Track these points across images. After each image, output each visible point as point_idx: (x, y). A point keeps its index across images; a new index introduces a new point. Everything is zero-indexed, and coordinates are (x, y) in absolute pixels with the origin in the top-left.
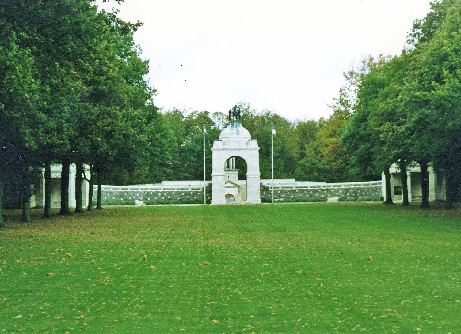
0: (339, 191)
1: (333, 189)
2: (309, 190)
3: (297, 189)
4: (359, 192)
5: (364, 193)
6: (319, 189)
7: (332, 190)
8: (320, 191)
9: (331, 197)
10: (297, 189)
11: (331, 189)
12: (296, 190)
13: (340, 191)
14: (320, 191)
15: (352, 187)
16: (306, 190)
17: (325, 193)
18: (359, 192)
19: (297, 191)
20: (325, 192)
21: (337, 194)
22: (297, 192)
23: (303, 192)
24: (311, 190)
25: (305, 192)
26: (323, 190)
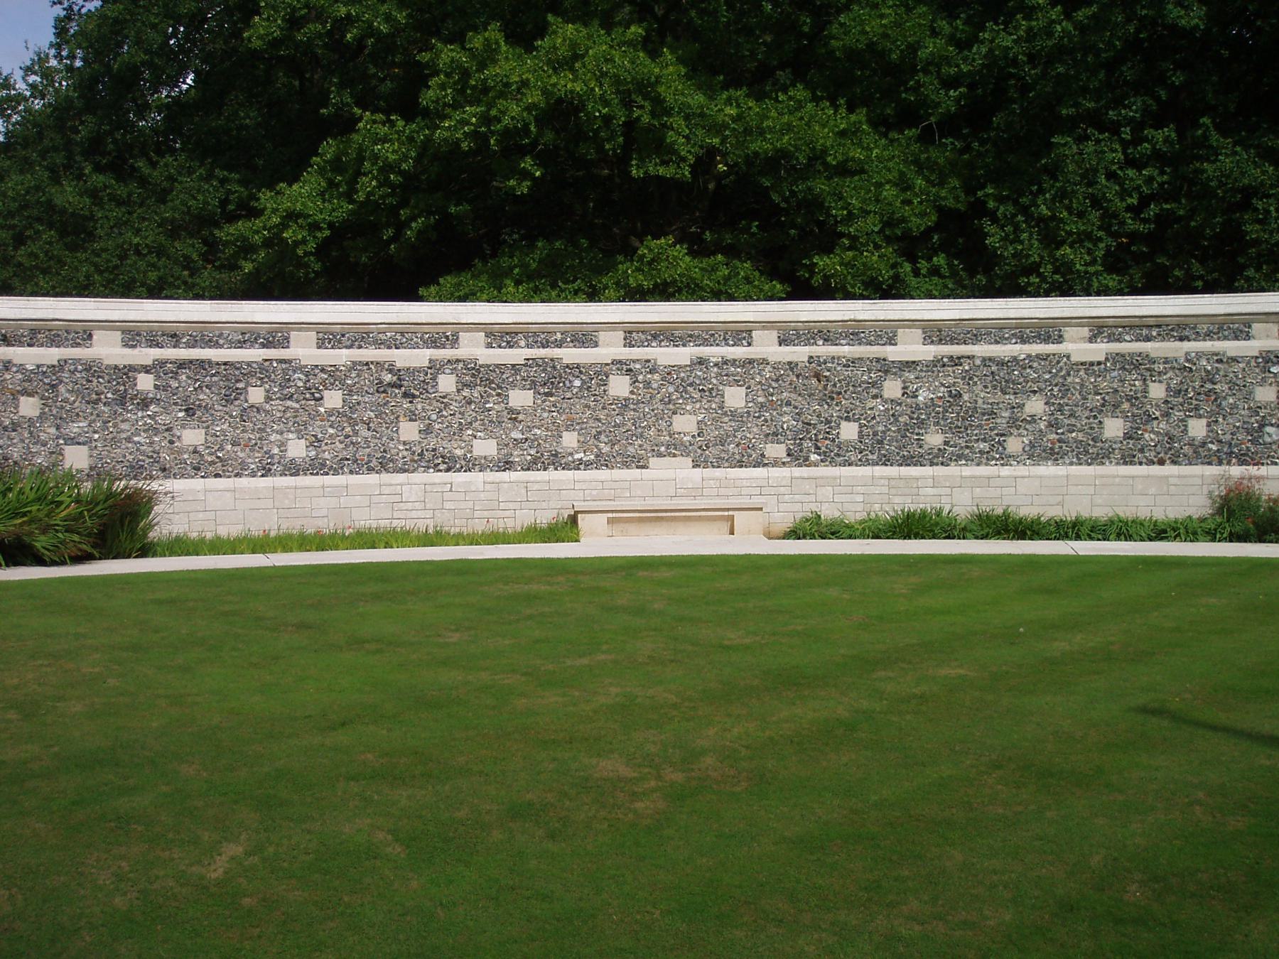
0: (712, 393)
1: (623, 366)
2: (310, 372)
3: (147, 355)
4: (1035, 406)
5: (1114, 428)
6: (436, 368)
7: (619, 386)
8: (447, 383)
9: (588, 465)
10: (147, 355)
11: (601, 373)
12: (127, 373)
13: (735, 397)
14: (447, 383)
15: (911, 348)
16: (262, 372)
17: (514, 416)
18: (1035, 406)
19: (145, 383)
20: (521, 398)
21: (685, 424)
22: (145, 403)
23: (232, 395)
24: (333, 376)
25: (256, 395)
26: (474, 374)
